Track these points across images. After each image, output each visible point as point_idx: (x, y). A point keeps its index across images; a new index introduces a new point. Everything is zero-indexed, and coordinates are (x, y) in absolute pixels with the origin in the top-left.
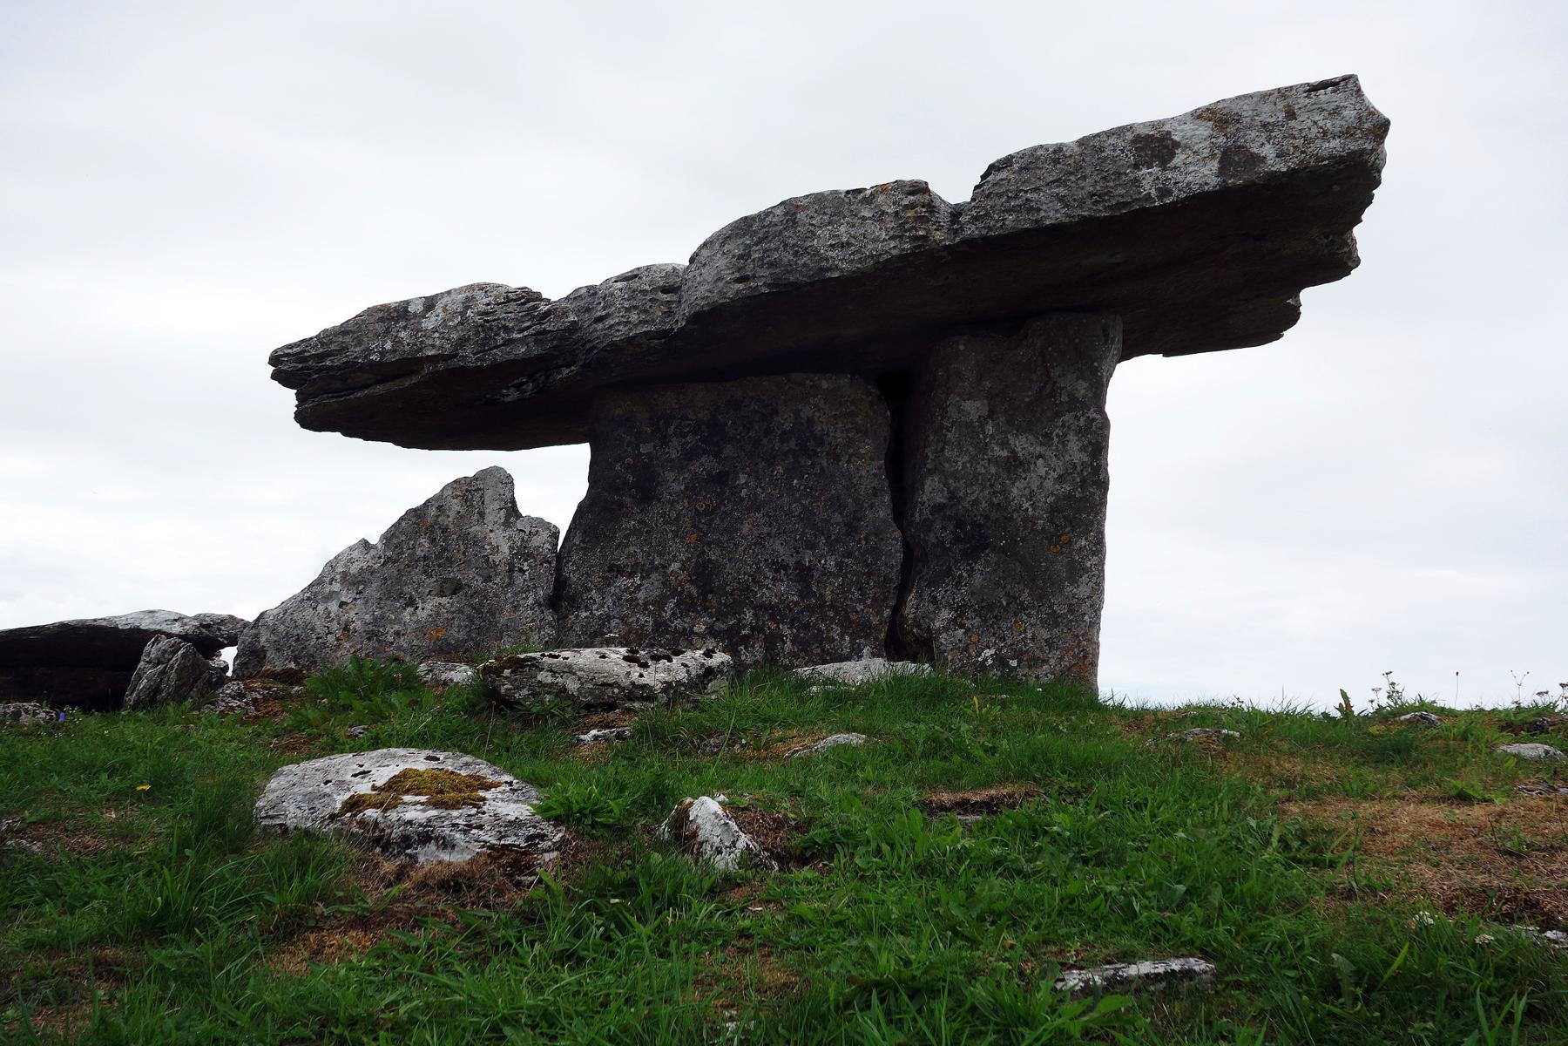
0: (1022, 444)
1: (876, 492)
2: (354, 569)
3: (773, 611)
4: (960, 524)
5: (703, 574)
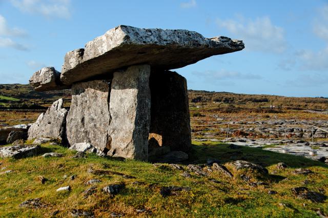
0: (124, 96)
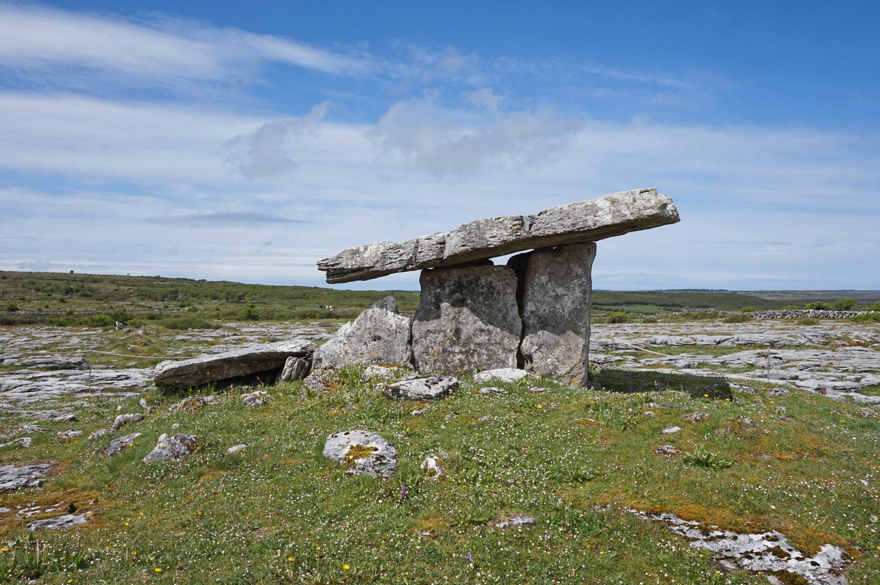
0: (560, 291)
1: (513, 306)
2: (348, 332)
3: (479, 345)
4: (540, 318)
5: (457, 332)
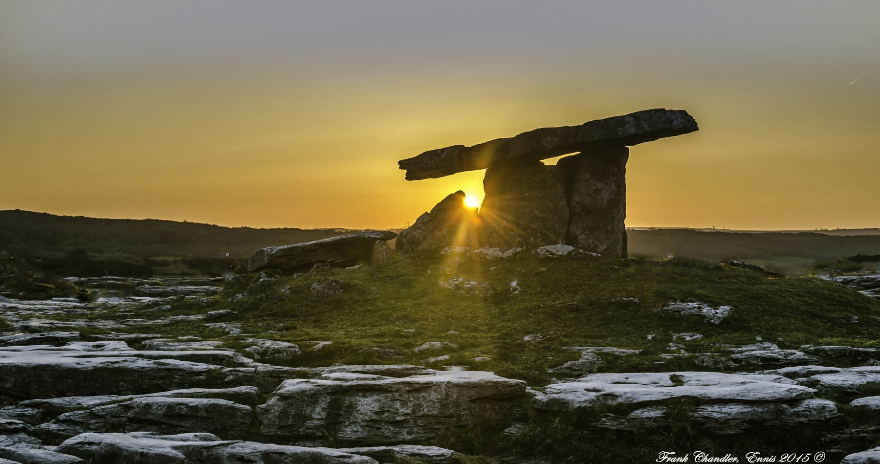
0: (600, 185)
